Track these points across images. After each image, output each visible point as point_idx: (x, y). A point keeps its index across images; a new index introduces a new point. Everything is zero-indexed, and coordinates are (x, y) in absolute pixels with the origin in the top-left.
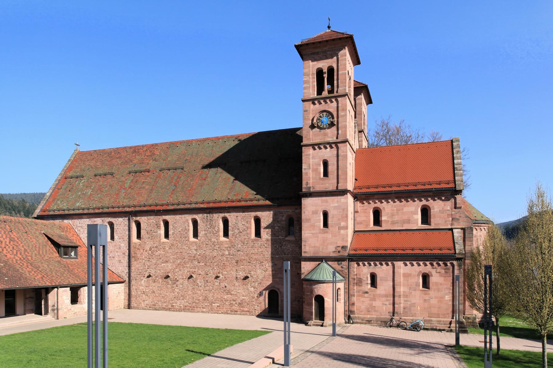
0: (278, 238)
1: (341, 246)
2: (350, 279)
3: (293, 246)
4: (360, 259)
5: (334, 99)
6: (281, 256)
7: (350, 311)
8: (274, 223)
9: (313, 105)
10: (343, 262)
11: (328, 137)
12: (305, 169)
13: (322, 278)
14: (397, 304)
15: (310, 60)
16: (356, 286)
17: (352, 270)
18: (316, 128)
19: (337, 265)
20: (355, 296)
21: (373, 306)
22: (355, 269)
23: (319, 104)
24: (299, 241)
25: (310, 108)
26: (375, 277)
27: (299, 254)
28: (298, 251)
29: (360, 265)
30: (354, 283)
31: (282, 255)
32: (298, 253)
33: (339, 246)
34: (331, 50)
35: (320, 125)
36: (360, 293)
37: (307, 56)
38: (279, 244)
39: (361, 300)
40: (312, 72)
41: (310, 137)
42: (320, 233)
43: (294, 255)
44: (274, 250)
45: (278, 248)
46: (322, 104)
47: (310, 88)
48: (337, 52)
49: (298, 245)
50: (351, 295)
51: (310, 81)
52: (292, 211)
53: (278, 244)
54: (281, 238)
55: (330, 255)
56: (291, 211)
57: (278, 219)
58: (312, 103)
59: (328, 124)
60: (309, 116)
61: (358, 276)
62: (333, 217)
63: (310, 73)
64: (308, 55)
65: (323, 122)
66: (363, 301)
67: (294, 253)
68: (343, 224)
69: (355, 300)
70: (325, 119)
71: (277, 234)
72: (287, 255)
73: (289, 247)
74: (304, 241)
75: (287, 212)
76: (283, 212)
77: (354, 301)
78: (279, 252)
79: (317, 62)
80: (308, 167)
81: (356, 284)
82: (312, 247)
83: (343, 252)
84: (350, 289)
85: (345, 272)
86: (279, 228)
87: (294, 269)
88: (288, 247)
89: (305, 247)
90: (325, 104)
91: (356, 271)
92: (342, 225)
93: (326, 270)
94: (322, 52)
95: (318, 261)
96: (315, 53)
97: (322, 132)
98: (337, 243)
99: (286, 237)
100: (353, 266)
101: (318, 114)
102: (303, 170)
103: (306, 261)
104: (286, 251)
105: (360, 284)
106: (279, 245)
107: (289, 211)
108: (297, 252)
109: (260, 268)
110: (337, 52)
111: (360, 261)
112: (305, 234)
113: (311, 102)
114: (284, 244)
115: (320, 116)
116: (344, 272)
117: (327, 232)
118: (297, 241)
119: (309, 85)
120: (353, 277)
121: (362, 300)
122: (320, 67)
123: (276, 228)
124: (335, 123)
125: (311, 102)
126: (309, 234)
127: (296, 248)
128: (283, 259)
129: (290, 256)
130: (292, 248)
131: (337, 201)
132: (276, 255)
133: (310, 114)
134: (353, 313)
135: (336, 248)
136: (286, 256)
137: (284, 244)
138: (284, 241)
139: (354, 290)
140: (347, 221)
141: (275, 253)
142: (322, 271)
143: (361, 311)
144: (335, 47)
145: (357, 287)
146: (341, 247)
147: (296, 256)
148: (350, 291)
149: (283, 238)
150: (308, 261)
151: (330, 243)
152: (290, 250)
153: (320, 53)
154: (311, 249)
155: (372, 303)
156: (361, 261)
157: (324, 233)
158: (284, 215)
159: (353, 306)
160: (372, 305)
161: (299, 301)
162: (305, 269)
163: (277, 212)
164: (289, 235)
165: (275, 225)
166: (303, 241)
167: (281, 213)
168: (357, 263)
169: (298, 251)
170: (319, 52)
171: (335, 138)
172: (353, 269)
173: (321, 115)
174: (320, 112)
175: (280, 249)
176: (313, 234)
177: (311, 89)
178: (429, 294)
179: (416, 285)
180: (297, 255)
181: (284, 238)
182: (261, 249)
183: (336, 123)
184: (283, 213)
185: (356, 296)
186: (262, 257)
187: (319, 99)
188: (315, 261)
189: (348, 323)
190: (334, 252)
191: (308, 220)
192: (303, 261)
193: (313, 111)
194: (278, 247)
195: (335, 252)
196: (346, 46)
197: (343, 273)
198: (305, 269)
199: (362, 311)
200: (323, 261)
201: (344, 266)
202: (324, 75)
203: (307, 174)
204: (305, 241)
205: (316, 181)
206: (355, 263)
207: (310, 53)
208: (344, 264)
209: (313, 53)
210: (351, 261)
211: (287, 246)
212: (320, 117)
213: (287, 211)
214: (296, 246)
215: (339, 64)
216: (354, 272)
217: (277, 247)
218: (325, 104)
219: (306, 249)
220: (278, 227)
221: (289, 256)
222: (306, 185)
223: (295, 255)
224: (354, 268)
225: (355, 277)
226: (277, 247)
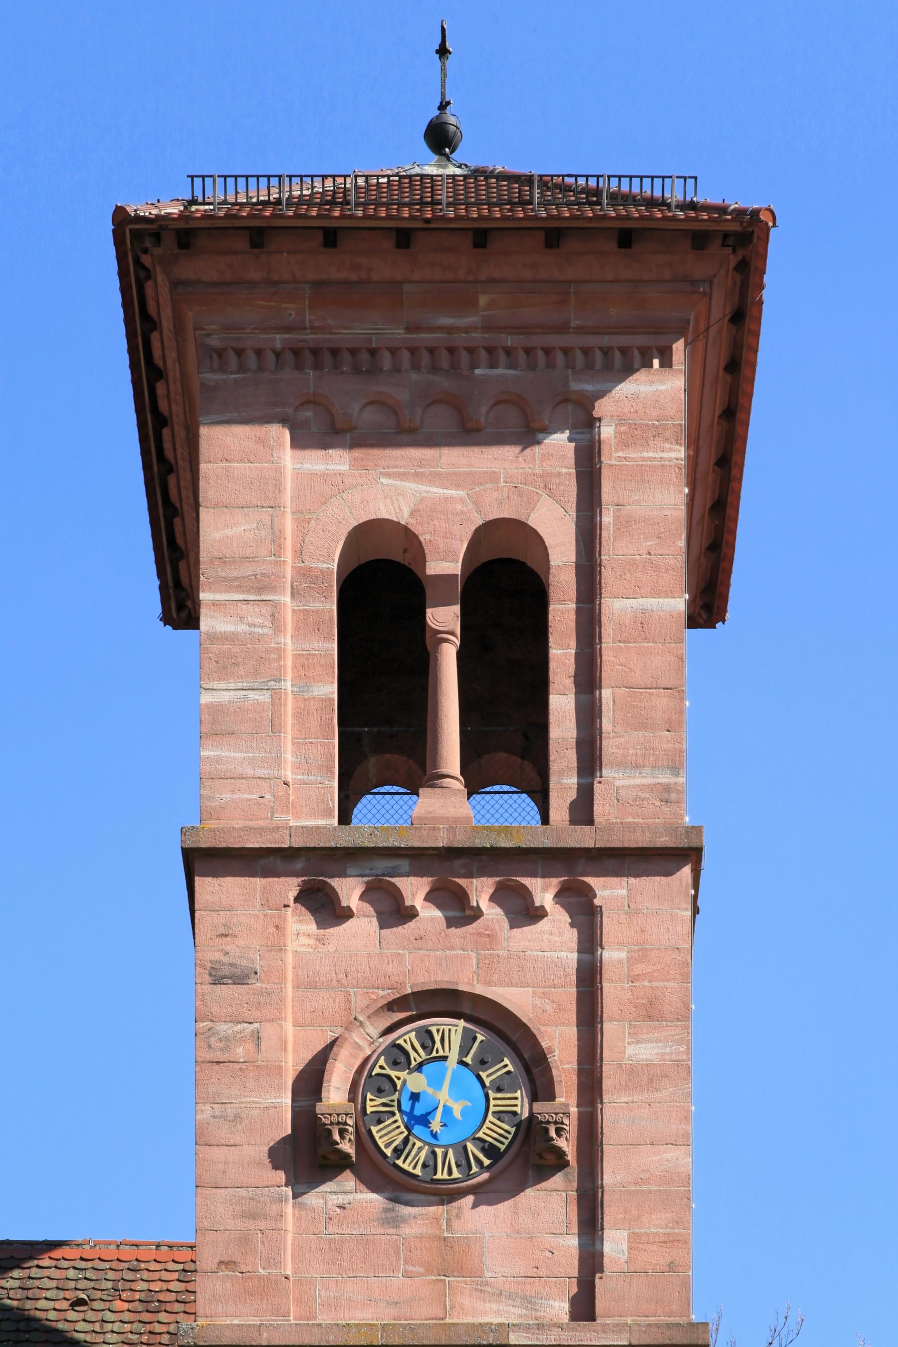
5: (555, 883)
9: (312, 927)
11: (482, 1289)
15: (283, 421)
18: (348, 1180)
23: (384, 924)
25: (281, 949)
34: (508, 351)
35: (398, 1152)
37: (242, 369)
40: (299, 553)
41: (273, 1261)
46: (412, 924)
47: (275, 727)
48: (582, 386)
51: (280, 652)
58: (296, 900)
59: (490, 1150)
60: (268, 1031)
63: (280, 564)
64: (252, 361)
65: (424, 1121)
70: (457, 1090)
79: (358, 453)
90: (451, 923)
94: (413, 350)
96: (335, 352)
97: (410, 1230)
101: (373, 1030)
110: (582, 386)
113: (290, 887)
115: (395, 1046)
119: (264, 697)
122: (384, 511)
124: (561, 1143)
125: (290, 887)
133: (277, 1019)
144: (562, 328)
153: (386, 361)
170: (373, 352)
171: (560, 1309)
173: (408, 1037)
174: (392, 1006)
177: (289, 734)
183: (567, 1145)
187: (382, 865)
193: (311, 985)
196: (680, 331)
202: (429, 612)
207: (279, 340)
209: (316, 352)
212: (395, 1064)
215: (607, 518)
218: (451, 923)
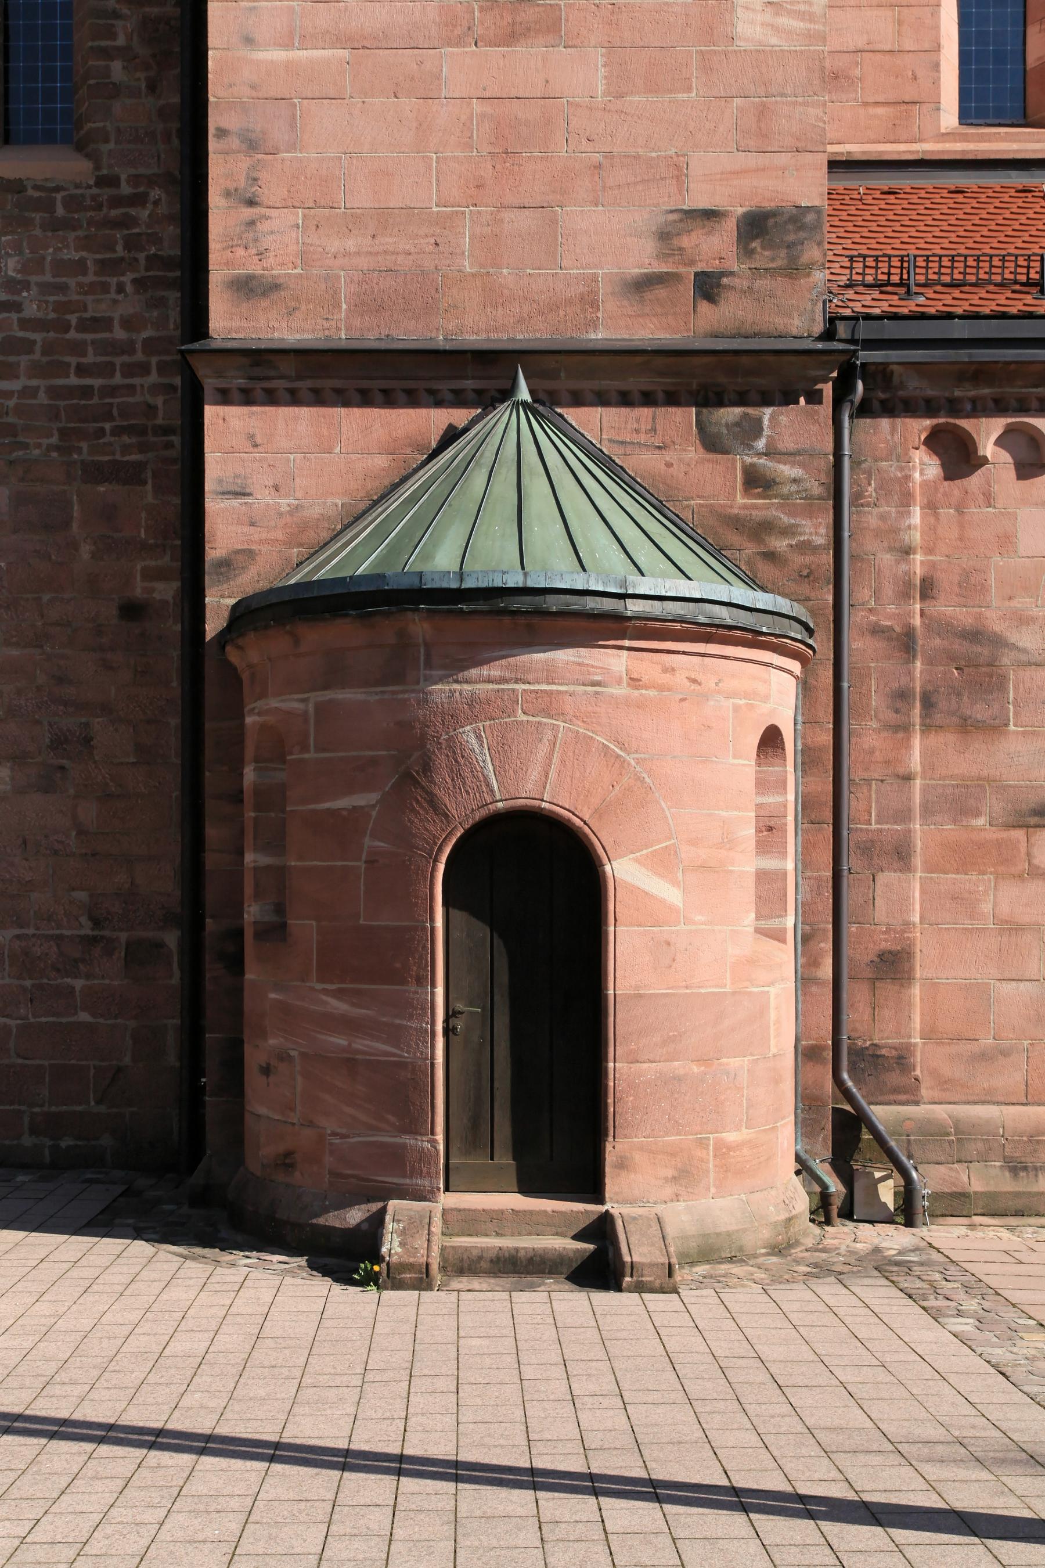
1: (741, 211)
2: (855, 643)
3: (61, 267)
4: (979, 374)
7: (857, 1053)
10: (768, 412)
16: (927, 728)
17: (872, 519)
19: (693, 452)
20: (918, 861)
22: (916, 516)
27: (139, 356)
28: (127, 324)
29: (985, 461)
30: (903, 695)
32: (128, 348)
33: (710, 215)
36: (981, 822)
39: (987, 908)
43: (82, 370)
49: (131, 244)
50: (867, 850)
55: (594, 324)
61: (946, 608)
66: (1011, 928)
67: (78, 348)
69: (916, 919)
74: (234, 143)
77: (908, 925)
81: (928, 703)
82: (354, 220)
83: (763, 284)
84: (854, 770)
85: (805, 547)
87: (86, 550)
89: (252, 223)
91: (931, 530)
95: (439, 404)
98: (680, 174)
100: (890, 468)
103: (272, 399)
105: (980, 712)
108: (119, 334)
111: (979, 409)
112: (249, 41)
116: (780, 544)
118: (117, 202)
120: (889, 614)
121: (1005, 910)
127: (105, 288)
130: (45, 288)
134: (894, 1078)
135: (664, 236)
139: (908, 778)
143: (984, 1057)
145: (936, 740)
146: (730, 226)
147: (112, 391)
148: (854, 804)
150: (295, 399)
152: (31, 310)
154: (334, 245)
156: (999, 407)
157: (511, 37)
159: (886, 988)
166: (222, 133)
168: (934, 441)
169: (127, 324)
172: (889, 509)
180: (118, 379)
185: (930, 868)
188: (389, 400)
189: (848, 1213)
190: (644, 284)
192: (225, 398)
195: (661, 292)
197: (771, 556)
198: (263, 499)
200: (507, 393)
201: (787, 470)
204: (252, 144)
206: (920, 427)
208: (787, 443)
210: (864, 410)
214: (108, 266)
216: (907, 551)
219: (266, 242)
221: (15, 385)
223: (97, 382)
224: (906, 500)
225: (917, 621)
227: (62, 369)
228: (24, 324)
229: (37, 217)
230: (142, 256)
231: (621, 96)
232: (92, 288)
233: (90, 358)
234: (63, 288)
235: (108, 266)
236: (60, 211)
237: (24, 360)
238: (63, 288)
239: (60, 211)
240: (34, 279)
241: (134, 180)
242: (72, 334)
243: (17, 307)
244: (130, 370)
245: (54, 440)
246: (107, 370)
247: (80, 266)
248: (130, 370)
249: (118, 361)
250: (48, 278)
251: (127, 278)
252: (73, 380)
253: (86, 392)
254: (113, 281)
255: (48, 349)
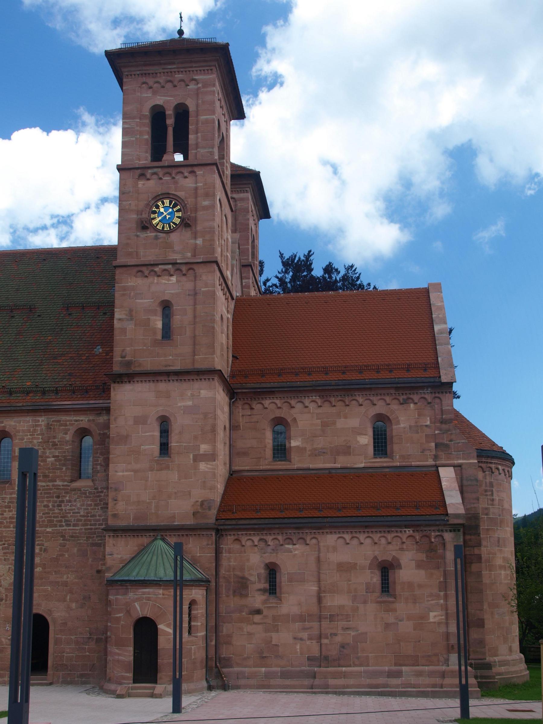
0: (53, 485)
1: (200, 500)
6: (58, 528)
8: (44, 449)
12: (120, 319)
13: (152, 575)
14: (327, 638)
21: (274, 643)
24: (102, 492)
26: (278, 574)
27: (101, 522)
28: (99, 516)
31: (61, 526)
32: (99, 520)
38: (56, 499)
42: (151, 469)
43: (91, 525)
44: (43, 514)
45: (50, 510)
49: (100, 501)
52: (89, 421)
53: (52, 499)
54: (61, 483)
56: (87, 419)
57: (55, 437)
62: (180, 433)
67: (90, 521)
68: (204, 448)
71: (51, 475)
72: (74, 525)
73: (78, 505)
75: (76, 421)
76: (68, 423)
78: (55, 519)
80: (127, 315)
86: (55, 460)
88: (75, 506)
92: (202, 452)
93: (165, 556)
99: (72, 481)
102: (115, 322)
104: (71, 516)
106: (56, 502)
107: (81, 419)
108: (98, 518)
109: (5, 560)
112: (116, 471)
114: (67, 498)
117: (167, 468)
123: (49, 460)
126: (127, 471)
127: (95, 509)
128: (62, 536)
129: (81, 529)
130: (85, 509)
131: (192, 395)
132: (46, 526)
136: (72, 528)
137: (67, 498)
138: (67, 493)
140: (213, 441)
141: (43, 521)
142: (155, 558)
147: (97, 529)
149: (66, 483)
151: (175, 493)
152: (82, 513)
155: (272, 637)
158: (69, 430)
160: (271, 641)
161: (98, 641)
162: (115, 556)
163: (53, 422)
164: (80, 478)
165: (47, 454)
166: (111, 488)
167: (61, 425)
175: (56, 511)
176: (136, 471)
178: (395, 610)
179: (367, 591)
180: (97, 527)
181: (69, 484)
182: (10, 511)
184: (66, 425)
186: (11, 531)
191: (125, 439)
194: (54, 506)
199: (248, 658)
203: (124, 331)
205: (145, 348)
211: (73, 505)
213: (78, 418)
217: (51, 507)
220: (54, 457)
222: (122, 357)
226: (49, 507)
227: (87, 525)
228: (81, 516)
229: (84, 495)
230: (102, 503)
231: (180, 480)
232: (93, 509)
233: (93, 522)
234: (88, 509)
235: (96, 505)
236: (88, 494)
237: (80, 523)
238: (88, 509)
239: (88, 494)
240: (82, 507)
241: (101, 488)
242: (89, 518)
243: (79, 513)
244: (100, 525)
245: (85, 539)
246: (95, 525)
247: (91, 505)
248: (100, 525)
249: (97, 523)
250: (85, 507)
251: (99, 507)
252: (89, 527)
253: (91, 529)
254: (97, 507)
255: (85, 520)
